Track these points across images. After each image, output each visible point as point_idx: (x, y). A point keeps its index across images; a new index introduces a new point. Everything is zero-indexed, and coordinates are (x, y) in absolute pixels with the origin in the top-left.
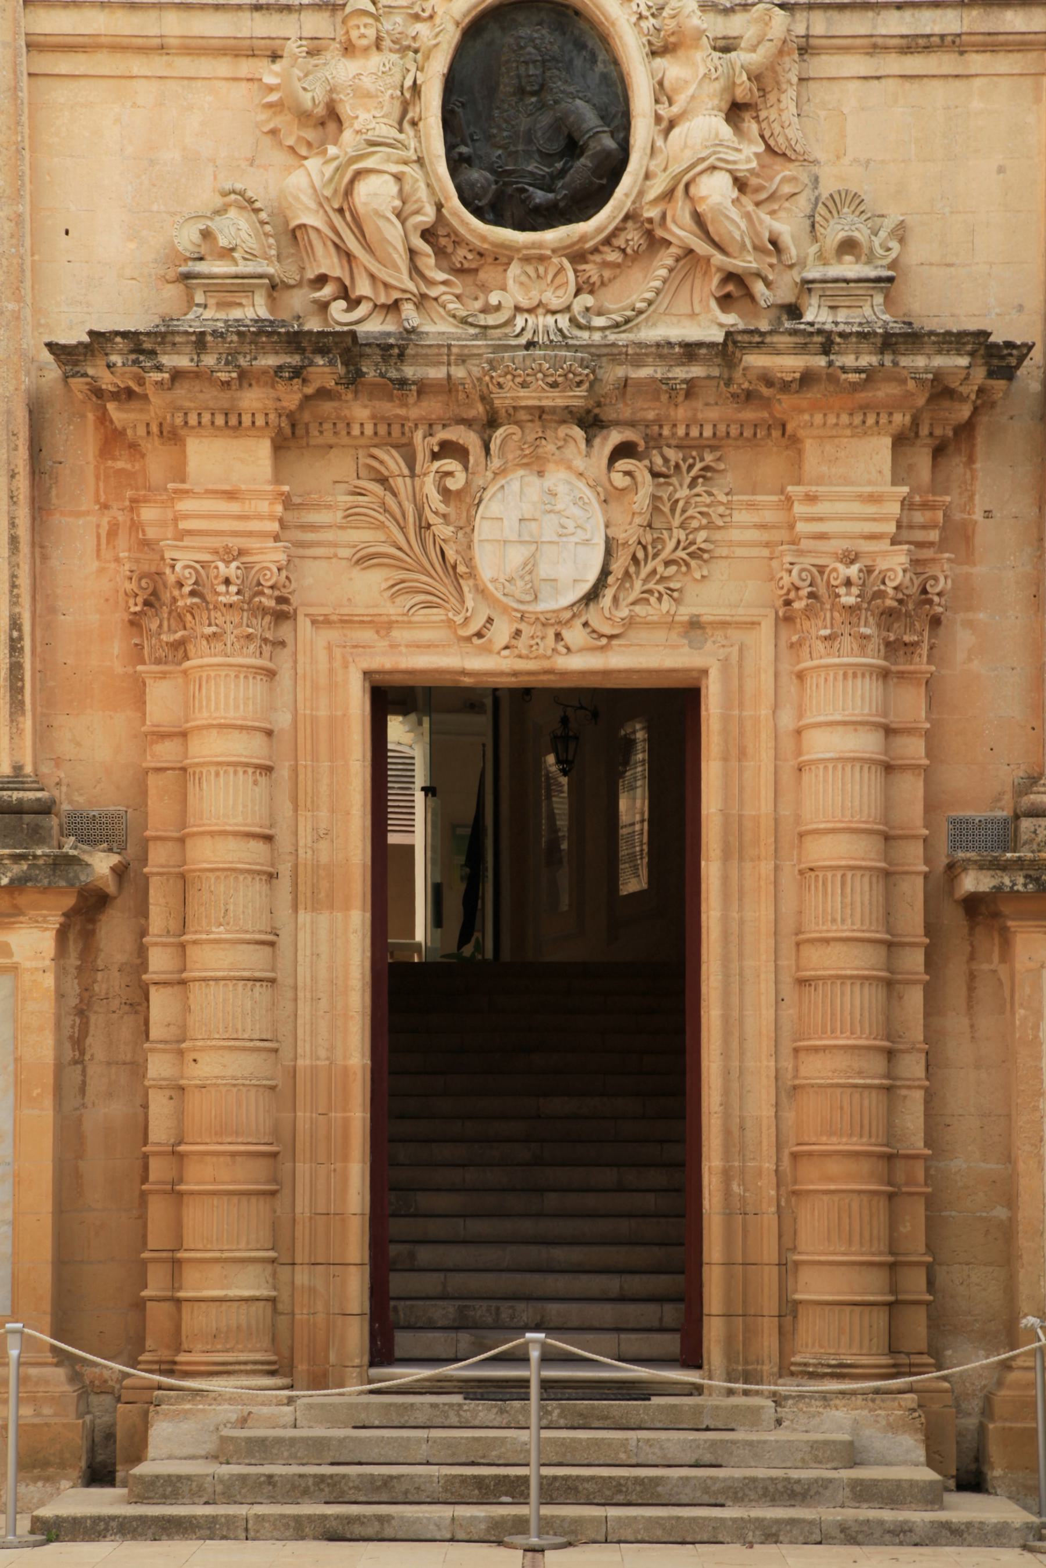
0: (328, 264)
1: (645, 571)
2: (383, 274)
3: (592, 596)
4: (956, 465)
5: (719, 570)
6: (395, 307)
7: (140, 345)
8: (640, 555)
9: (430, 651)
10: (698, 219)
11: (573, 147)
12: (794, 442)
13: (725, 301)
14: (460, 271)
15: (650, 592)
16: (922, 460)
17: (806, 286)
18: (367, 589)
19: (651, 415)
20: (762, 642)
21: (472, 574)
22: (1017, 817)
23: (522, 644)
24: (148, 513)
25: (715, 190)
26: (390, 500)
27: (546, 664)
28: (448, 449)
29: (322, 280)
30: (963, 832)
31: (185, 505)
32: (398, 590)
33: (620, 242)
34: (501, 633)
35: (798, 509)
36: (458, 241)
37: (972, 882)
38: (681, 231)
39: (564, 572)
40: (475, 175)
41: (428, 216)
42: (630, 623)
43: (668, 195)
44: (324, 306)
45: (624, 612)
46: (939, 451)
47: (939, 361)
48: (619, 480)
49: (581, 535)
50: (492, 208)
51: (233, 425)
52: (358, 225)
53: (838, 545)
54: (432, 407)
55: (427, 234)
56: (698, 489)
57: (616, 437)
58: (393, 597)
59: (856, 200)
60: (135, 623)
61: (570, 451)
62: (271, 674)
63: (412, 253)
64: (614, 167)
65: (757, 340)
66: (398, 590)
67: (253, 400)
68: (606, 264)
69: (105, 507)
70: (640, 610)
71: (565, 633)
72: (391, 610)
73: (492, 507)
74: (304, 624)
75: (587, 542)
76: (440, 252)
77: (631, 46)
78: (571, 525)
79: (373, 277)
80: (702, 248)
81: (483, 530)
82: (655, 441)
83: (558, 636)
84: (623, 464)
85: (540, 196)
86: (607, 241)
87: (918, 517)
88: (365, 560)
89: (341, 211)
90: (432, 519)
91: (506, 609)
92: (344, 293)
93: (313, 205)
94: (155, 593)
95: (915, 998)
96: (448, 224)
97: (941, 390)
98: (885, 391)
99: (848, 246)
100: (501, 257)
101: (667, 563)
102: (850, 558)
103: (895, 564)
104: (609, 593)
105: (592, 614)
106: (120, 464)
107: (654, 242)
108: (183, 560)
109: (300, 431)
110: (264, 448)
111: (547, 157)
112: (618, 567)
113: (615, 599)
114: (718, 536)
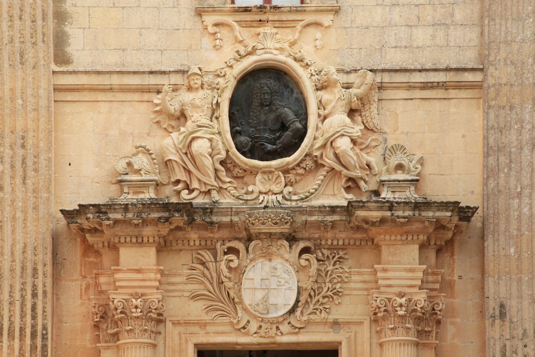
0: (181, 175)
1: (314, 301)
2: (204, 179)
3: (292, 311)
4: (446, 257)
5: (346, 300)
6: (209, 192)
8: (312, 294)
9: (222, 336)
10: (336, 156)
11: (284, 127)
12: (377, 247)
13: (348, 189)
14: (236, 178)
15: (317, 309)
16: (432, 255)
17: (382, 183)
18: (197, 310)
19: (317, 236)
20: (365, 332)
21: (241, 302)
23: (262, 332)
24: (102, 280)
26: (206, 272)
27: (272, 340)
28: (232, 250)
29: (178, 182)
31: (118, 276)
32: (209, 309)
33: (303, 165)
34: (253, 327)
35: (379, 274)
36: (236, 165)
38: (329, 160)
39: (280, 301)
40: (243, 139)
41: (223, 155)
42: (308, 322)
43: (324, 146)
44: (179, 193)
45: (305, 318)
46: (439, 251)
47: (438, 214)
48: (303, 263)
49: (287, 286)
50: (250, 153)
52: (193, 159)
53: (397, 290)
54: (225, 233)
55: (222, 163)
56: (337, 266)
57: (302, 245)
58: (207, 312)
59: (402, 148)
60: (96, 326)
61: (282, 251)
63: (216, 170)
64: (301, 135)
65: (362, 205)
66: (209, 309)
67: (148, 231)
68: (297, 174)
69: (85, 277)
70: (312, 317)
71: (281, 327)
72: (207, 318)
73: (249, 274)
74: (169, 324)
75: (290, 289)
76: (228, 170)
78: (283, 281)
79: (199, 180)
80: (338, 167)
81: (246, 284)
82: (319, 247)
83: (278, 328)
84: (305, 256)
85: (270, 147)
86: (298, 165)
87: (430, 278)
88: (195, 297)
89: (186, 154)
90: (224, 279)
91: (255, 317)
92: (187, 187)
93: (174, 151)
94: (105, 313)
96: (231, 158)
97: (439, 226)
98: (416, 226)
99: (400, 167)
100: (253, 172)
101: (324, 297)
102: (401, 295)
103: (421, 298)
104: (299, 310)
105: (292, 319)
106: (91, 259)
107: (318, 165)
108: (117, 299)
109: (168, 244)
110: (152, 251)
111: (273, 131)
112: (303, 299)
113: (302, 312)
114: (345, 286)
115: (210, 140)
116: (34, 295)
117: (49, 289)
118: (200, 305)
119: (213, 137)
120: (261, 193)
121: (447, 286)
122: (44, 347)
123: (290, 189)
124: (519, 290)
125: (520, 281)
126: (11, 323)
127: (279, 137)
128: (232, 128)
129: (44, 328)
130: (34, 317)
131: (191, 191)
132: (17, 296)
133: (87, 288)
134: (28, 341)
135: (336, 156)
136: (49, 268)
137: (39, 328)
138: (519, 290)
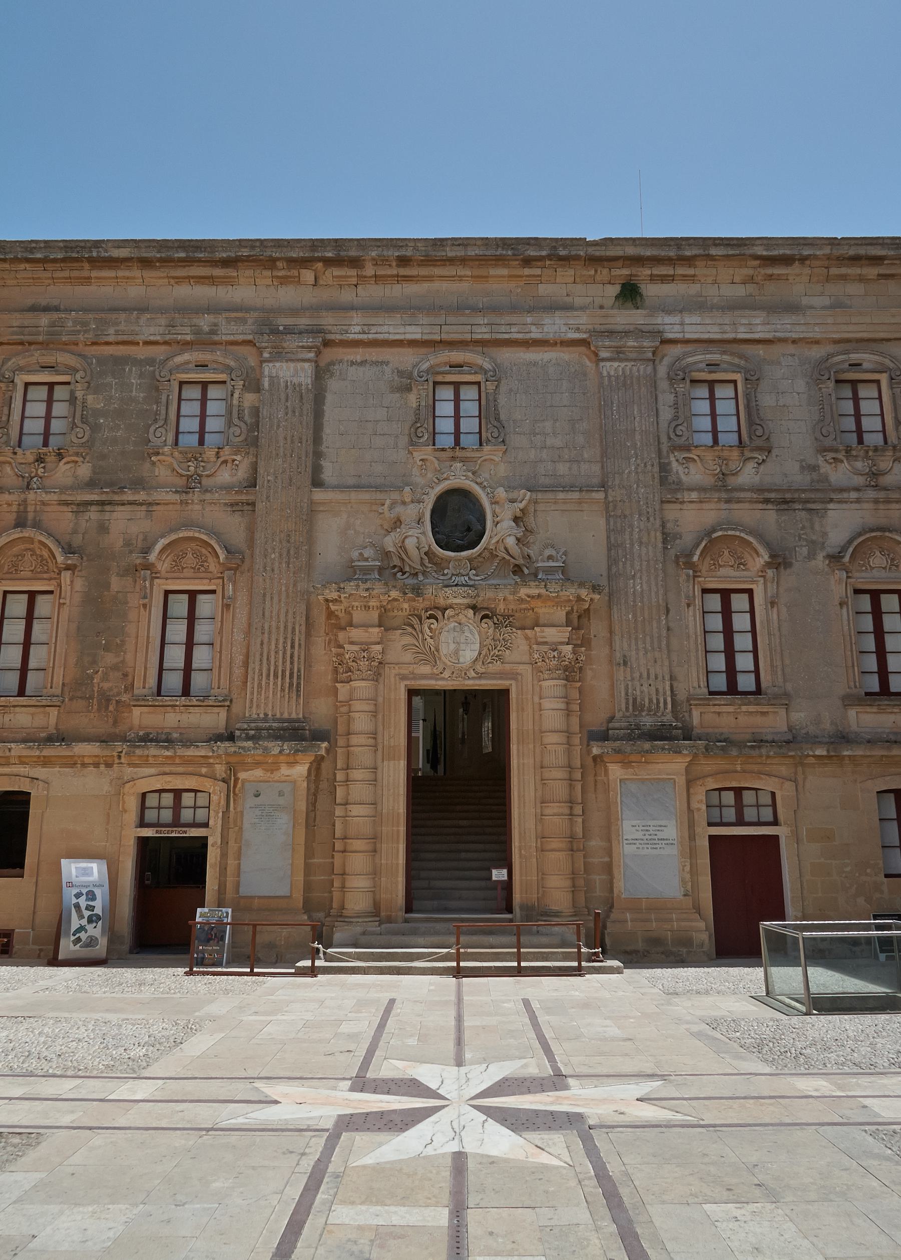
2: (413, 565)
11: (469, 529)
13: (515, 573)
29: (395, 566)
40: (438, 536)
41: (427, 549)
44: (395, 574)
84: (484, 620)
99: (550, 558)
115: (418, 538)
116: (293, 647)
117: (303, 643)
120: (453, 575)
121: (586, 642)
122: (299, 684)
123: (474, 572)
124: (637, 644)
125: (636, 639)
126: (276, 666)
127: (466, 536)
128: (433, 529)
129: (299, 671)
130: (292, 663)
131: (404, 573)
132: (281, 646)
133: (329, 643)
134: (288, 680)
135: (506, 549)
136: (303, 627)
137: (296, 670)
138: (637, 644)
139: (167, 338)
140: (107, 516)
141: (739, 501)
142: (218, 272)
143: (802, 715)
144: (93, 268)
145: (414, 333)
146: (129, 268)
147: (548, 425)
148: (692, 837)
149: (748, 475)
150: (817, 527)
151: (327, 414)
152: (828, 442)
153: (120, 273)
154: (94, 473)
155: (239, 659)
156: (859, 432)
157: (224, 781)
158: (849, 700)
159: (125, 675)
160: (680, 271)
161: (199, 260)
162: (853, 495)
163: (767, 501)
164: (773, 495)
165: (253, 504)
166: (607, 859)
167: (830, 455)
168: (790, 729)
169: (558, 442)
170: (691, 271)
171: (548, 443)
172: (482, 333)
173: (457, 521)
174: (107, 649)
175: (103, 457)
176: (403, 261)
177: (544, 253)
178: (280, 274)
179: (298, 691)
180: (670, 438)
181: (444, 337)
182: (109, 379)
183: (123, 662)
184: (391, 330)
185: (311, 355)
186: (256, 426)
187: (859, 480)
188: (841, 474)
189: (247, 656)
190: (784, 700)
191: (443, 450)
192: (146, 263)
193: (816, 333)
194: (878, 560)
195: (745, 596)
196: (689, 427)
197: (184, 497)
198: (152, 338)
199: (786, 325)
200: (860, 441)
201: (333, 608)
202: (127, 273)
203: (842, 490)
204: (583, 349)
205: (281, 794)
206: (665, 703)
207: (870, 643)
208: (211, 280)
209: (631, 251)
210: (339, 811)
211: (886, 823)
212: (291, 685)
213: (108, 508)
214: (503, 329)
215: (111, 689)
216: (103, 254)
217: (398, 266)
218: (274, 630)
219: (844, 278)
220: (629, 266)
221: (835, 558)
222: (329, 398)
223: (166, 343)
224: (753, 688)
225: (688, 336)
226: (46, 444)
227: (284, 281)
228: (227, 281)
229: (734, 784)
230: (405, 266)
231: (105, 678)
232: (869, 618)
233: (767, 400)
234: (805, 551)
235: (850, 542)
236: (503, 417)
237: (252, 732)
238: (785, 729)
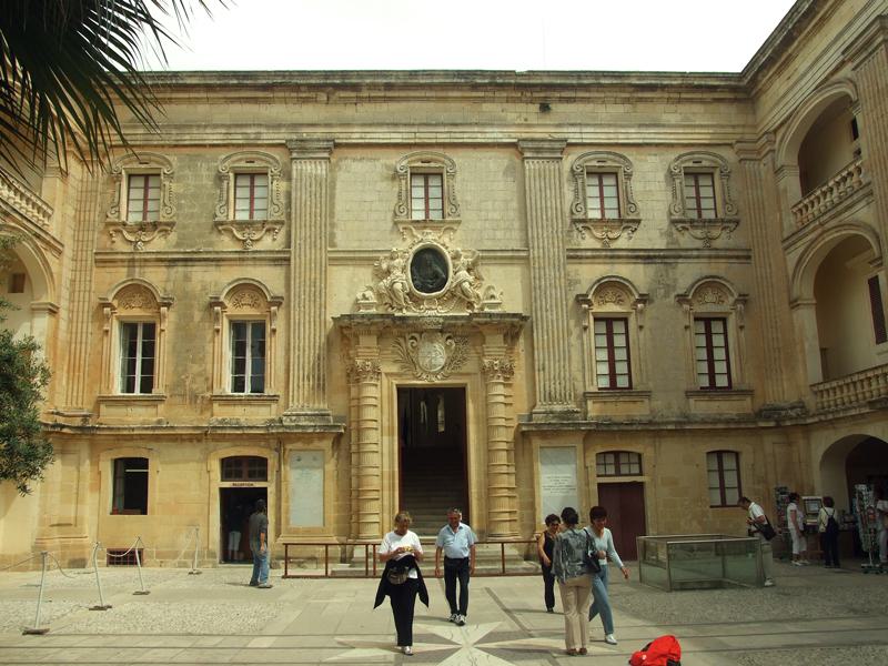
5: (468, 363)
7: (350, 317)
13: (468, 308)
16: (509, 341)
18: (394, 369)
22: (531, 414)
24: (351, 352)
25: (466, 285)
28: (413, 338)
30: (520, 417)
37: (524, 429)
41: (408, 291)
42: (451, 374)
46: (512, 338)
51: (369, 333)
54: (409, 329)
55: (408, 294)
57: (448, 335)
59: (493, 288)
60: (348, 375)
62: (376, 385)
64: (445, 281)
74: (383, 375)
77: (449, 257)
81: (420, 355)
82: (455, 336)
88: (396, 361)
95: (513, 453)
100: (423, 299)
107: (454, 296)
110: (375, 337)
118: (399, 365)
119: (402, 280)
139: (225, 142)
140: (189, 269)
141: (619, 257)
142: (260, 94)
143: (659, 402)
144: (172, 91)
145: (396, 138)
146: (198, 91)
147: (490, 203)
148: (587, 484)
149: (623, 241)
150: (671, 274)
151: (338, 196)
152: (676, 217)
153: (192, 95)
154: (179, 238)
155: (283, 367)
156: (699, 209)
157: (276, 450)
158: (689, 394)
159: (207, 379)
160: (581, 94)
161: (247, 85)
162: (695, 253)
163: (637, 257)
164: (642, 254)
165: (288, 260)
166: (531, 500)
167: (679, 226)
168: (652, 411)
169: (496, 216)
170: (587, 95)
171: (490, 217)
172: (443, 138)
173: (429, 269)
174: (193, 361)
175: (185, 227)
176: (389, 87)
177: (487, 81)
178: (304, 95)
179: (324, 390)
180: (572, 213)
181: (417, 141)
182: (187, 172)
183: (205, 370)
184: (381, 136)
185: (326, 155)
186: (289, 205)
187: (699, 244)
188: (686, 240)
189: (288, 366)
190: (646, 394)
191: (418, 221)
192: (209, 88)
193: (671, 139)
194: (710, 297)
195: (623, 323)
196: (585, 205)
197: (242, 256)
198: (215, 142)
199: (651, 135)
200: (700, 215)
201: (345, 332)
202: (196, 95)
203: (687, 250)
204: (512, 150)
205: (315, 459)
206: (570, 396)
207: (703, 354)
208: (255, 100)
209: (546, 80)
210: (353, 471)
211: (712, 473)
212: (319, 385)
213: (190, 263)
214: (458, 135)
215: (197, 389)
216: (181, 82)
217: (385, 90)
218: (307, 349)
219: (691, 101)
220: (546, 91)
221: (682, 299)
222: (339, 185)
223: (225, 145)
224: (627, 385)
225: (584, 141)
226: (145, 218)
227: (305, 100)
228: (267, 101)
229: (614, 449)
230: (389, 90)
231: (193, 381)
232: (704, 337)
233: (636, 186)
234: (662, 291)
235: (693, 286)
236: (458, 198)
237: (294, 418)
238: (648, 413)
